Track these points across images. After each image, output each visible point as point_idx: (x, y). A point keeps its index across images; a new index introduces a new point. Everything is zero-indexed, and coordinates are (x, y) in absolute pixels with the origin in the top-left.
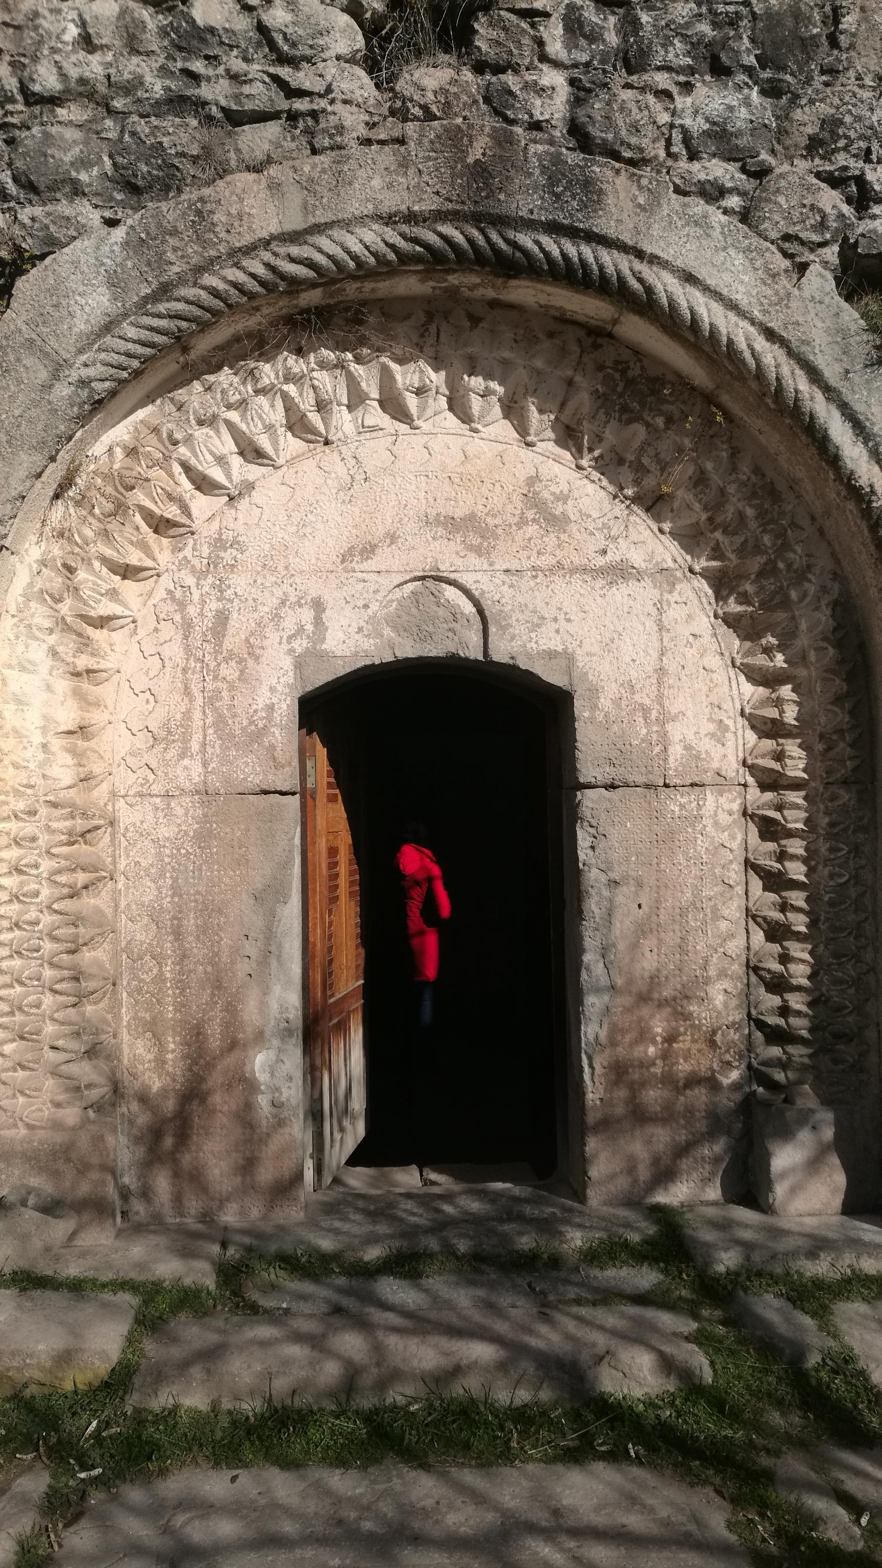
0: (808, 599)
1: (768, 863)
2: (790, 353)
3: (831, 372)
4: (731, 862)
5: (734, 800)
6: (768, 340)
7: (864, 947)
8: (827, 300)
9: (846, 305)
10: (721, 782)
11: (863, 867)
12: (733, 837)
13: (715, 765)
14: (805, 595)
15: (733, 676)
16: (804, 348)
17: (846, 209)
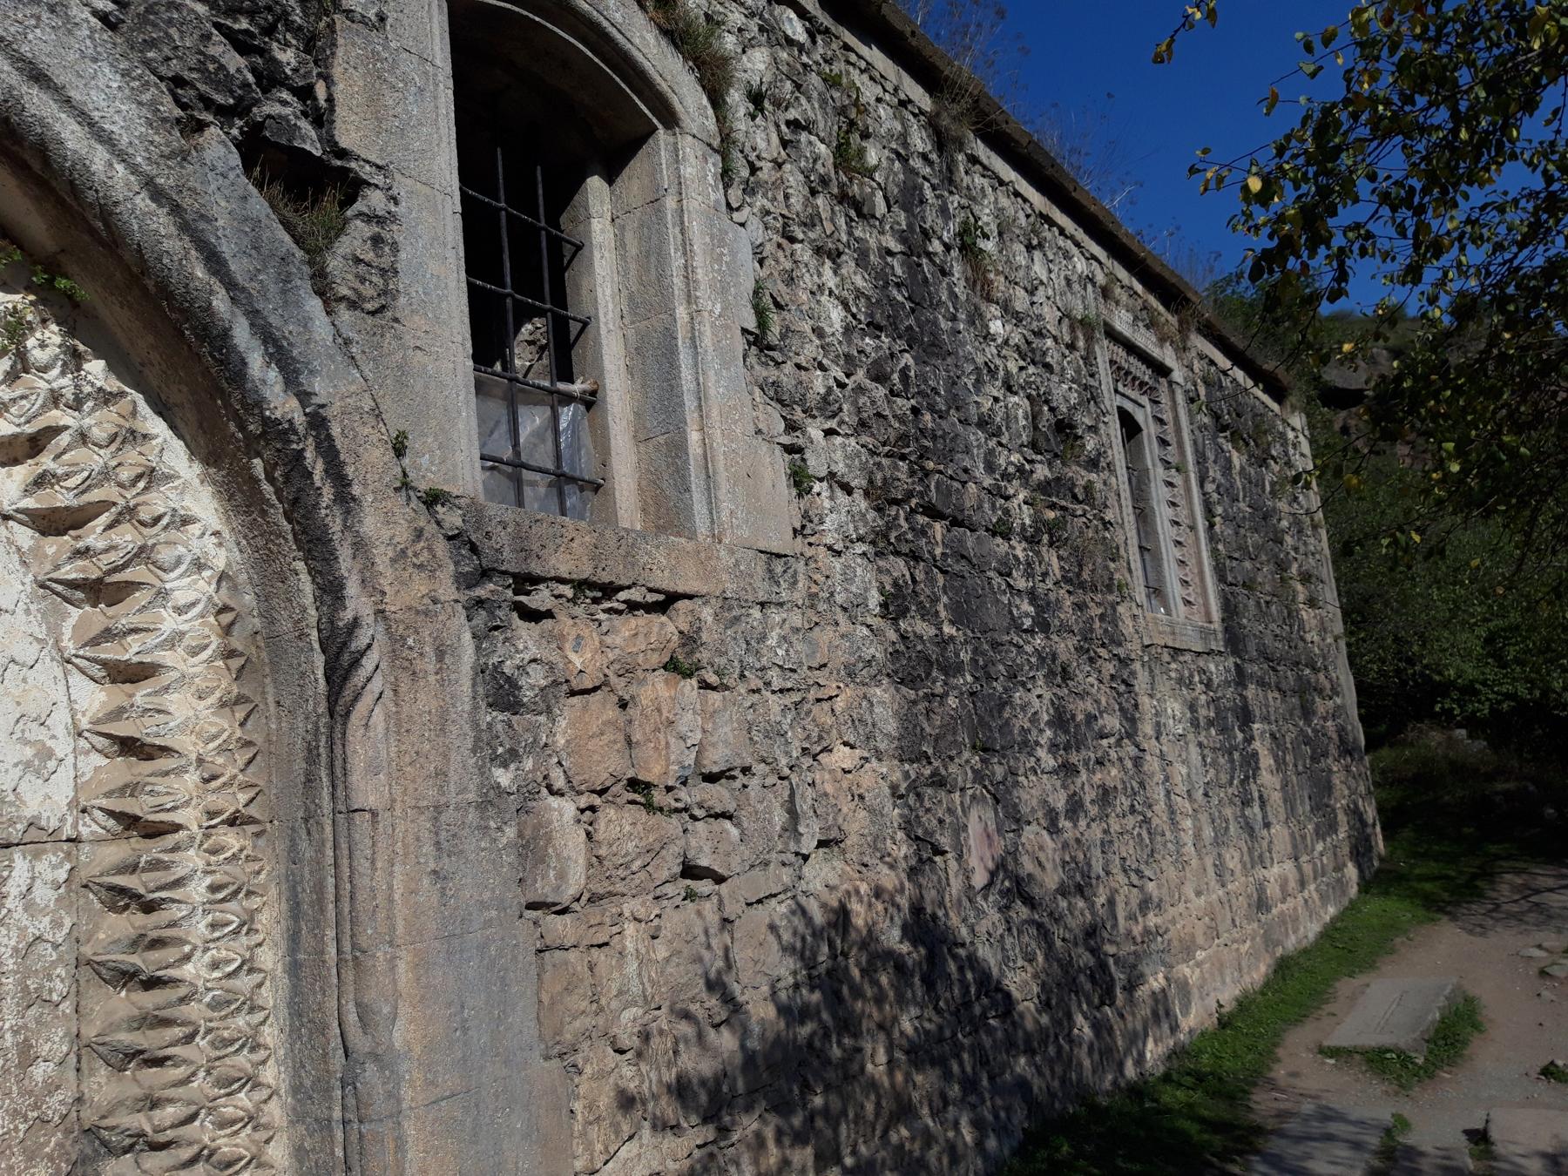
0: (183, 567)
1: (113, 957)
2: (185, 227)
3: (238, 268)
4: (54, 964)
5: (54, 867)
6: (153, 199)
7: (264, 1062)
8: (232, 176)
9: (255, 191)
10: (36, 838)
11: (260, 945)
12: (57, 924)
13: (28, 813)
14: (178, 562)
15: (60, 675)
16: (202, 225)
17: (250, 78)
